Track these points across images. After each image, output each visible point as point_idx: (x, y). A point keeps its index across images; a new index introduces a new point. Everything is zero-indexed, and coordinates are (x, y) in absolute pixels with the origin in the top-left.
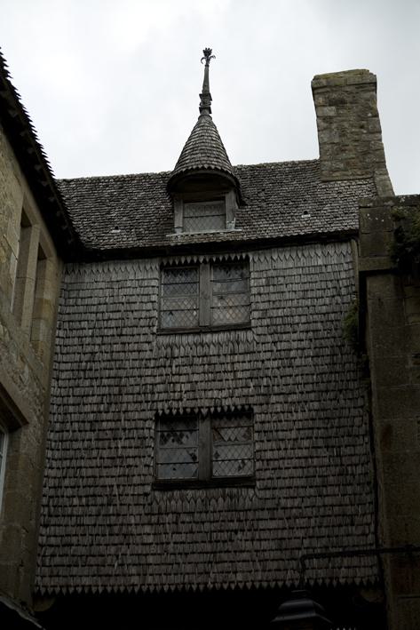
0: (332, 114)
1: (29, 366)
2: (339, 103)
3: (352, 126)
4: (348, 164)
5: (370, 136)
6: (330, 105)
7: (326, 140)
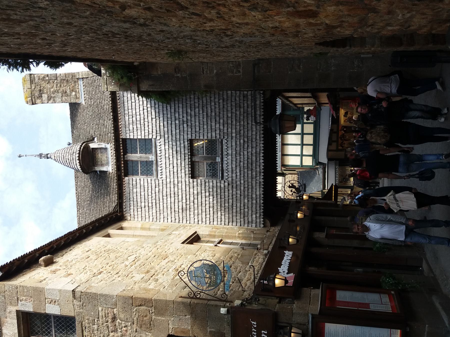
1: (173, 231)
2: (41, 92)
4: (73, 91)
5: (58, 79)
7: (60, 100)
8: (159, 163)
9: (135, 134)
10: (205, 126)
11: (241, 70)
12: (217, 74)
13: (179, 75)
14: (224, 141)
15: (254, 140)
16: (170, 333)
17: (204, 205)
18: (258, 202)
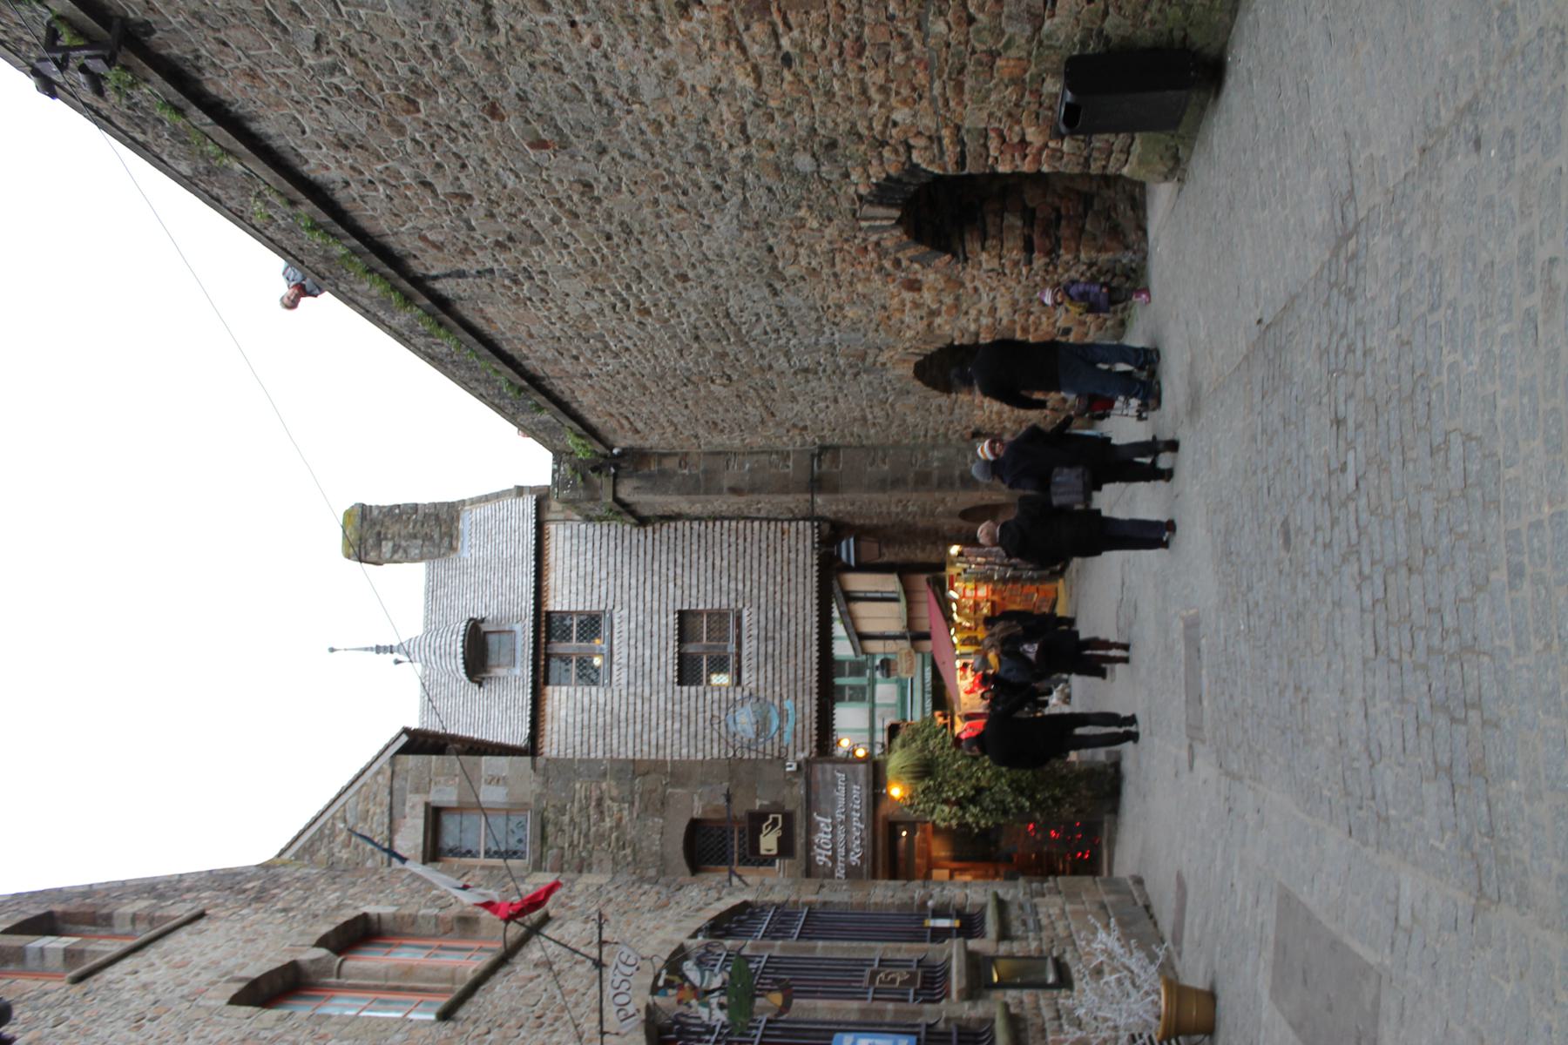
0: (390, 544)
3: (406, 527)
6: (380, 545)
8: (616, 658)
10: (709, 587)
11: (791, 464)
12: (751, 470)
13: (686, 471)
14: (745, 613)
15: (800, 610)
16: (697, 813)
17: (700, 737)
18: (807, 726)
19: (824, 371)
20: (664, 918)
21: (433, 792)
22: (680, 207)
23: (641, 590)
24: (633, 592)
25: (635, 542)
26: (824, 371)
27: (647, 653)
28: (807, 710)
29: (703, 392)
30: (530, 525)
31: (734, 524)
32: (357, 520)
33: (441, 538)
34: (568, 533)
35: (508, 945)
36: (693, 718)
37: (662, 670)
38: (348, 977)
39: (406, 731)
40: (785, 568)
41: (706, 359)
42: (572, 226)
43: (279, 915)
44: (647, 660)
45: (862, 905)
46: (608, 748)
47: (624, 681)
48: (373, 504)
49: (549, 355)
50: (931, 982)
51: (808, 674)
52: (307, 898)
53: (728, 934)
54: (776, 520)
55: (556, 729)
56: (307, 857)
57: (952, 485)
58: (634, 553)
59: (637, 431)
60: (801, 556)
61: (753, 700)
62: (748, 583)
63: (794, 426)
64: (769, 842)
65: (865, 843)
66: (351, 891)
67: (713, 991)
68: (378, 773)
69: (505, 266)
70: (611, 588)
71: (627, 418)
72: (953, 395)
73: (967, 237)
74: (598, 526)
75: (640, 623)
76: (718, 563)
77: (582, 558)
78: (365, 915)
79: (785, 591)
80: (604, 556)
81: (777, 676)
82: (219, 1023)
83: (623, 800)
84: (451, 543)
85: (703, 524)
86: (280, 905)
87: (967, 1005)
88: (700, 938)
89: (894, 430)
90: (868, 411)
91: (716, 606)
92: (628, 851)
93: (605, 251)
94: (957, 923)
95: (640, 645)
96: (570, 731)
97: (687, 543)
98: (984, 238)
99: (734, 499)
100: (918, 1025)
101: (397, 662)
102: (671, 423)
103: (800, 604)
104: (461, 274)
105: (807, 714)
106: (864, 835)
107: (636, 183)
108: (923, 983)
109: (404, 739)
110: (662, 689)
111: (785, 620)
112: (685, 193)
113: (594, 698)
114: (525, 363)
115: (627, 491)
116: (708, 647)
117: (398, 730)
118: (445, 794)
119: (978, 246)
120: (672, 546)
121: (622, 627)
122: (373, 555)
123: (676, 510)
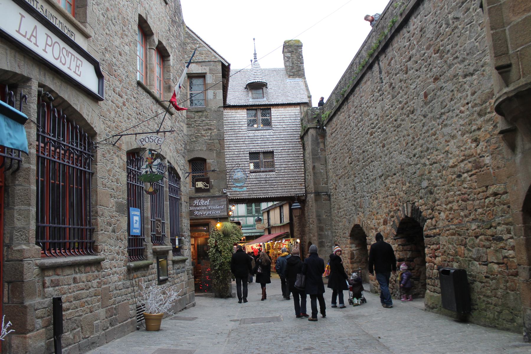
0: (290, 56)
3: (296, 60)
8: (257, 132)
9: (274, 117)
10: (282, 161)
11: (324, 185)
12: (321, 172)
13: (319, 151)
14: (274, 173)
16: (208, 161)
17: (233, 161)
18: (238, 195)
19: (355, 195)
20: (174, 152)
21: (210, 75)
22: (407, 144)
23: (279, 138)
24: (279, 136)
25: (295, 136)
26: (355, 195)
27: (259, 142)
28: (243, 195)
29: (346, 155)
30: (299, 101)
31: (303, 168)
32: (297, 44)
33: (293, 72)
34: (297, 114)
35: (162, 102)
36: (239, 158)
37: (254, 147)
38: (149, 52)
39: (229, 65)
40: (289, 185)
41: (357, 155)
42: (399, 108)
43: (168, 28)
44: (257, 142)
45: (181, 216)
46: (228, 131)
47: (249, 135)
48: (303, 49)
49: (355, 103)
50: (158, 239)
51: (255, 195)
52: (174, 37)
53: (170, 173)
54: (305, 182)
55: (233, 114)
56: (187, 36)
57: (320, 239)
58: (292, 136)
59: (332, 134)
60: (294, 190)
61: (246, 177)
62: (284, 173)
63: (336, 186)
64: (200, 185)
65: (201, 216)
66: (177, 51)
67: (151, 169)
68: (215, 57)
69: (384, 87)
70: (280, 129)
71: (336, 131)
72: (349, 238)
73: (403, 240)
74: (299, 123)
75: (268, 139)
76: (290, 163)
77: (289, 119)
78: (169, 56)
79: (282, 186)
80: (290, 126)
81: (254, 185)
82: (133, 11)
83: (211, 137)
84: (291, 75)
85: (302, 158)
86: (171, 28)
87: (151, 251)
88: (168, 164)
89: (337, 219)
90: (343, 210)
91: (276, 164)
92: (195, 139)
93: (391, 120)
94: (177, 247)
95: (262, 139)
96: (232, 118)
97: (296, 153)
98: (403, 245)
99: (311, 167)
100: (144, 236)
101: (251, 61)
102: (335, 145)
103: (278, 191)
104: (380, 72)
105: (242, 195)
106: (204, 216)
107: (414, 128)
108: (158, 237)
109: (227, 64)
110: (248, 147)
111: (273, 186)
112: (412, 145)
113: (243, 125)
114: (352, 95)
115: (312, 132)
116: (262, 161)
117: (229, 62)
118: (209, 79)
119: (400, 243)
120: (294, 148)
121: (267, 133)
122: (286, 50)
123: (306, 149)
